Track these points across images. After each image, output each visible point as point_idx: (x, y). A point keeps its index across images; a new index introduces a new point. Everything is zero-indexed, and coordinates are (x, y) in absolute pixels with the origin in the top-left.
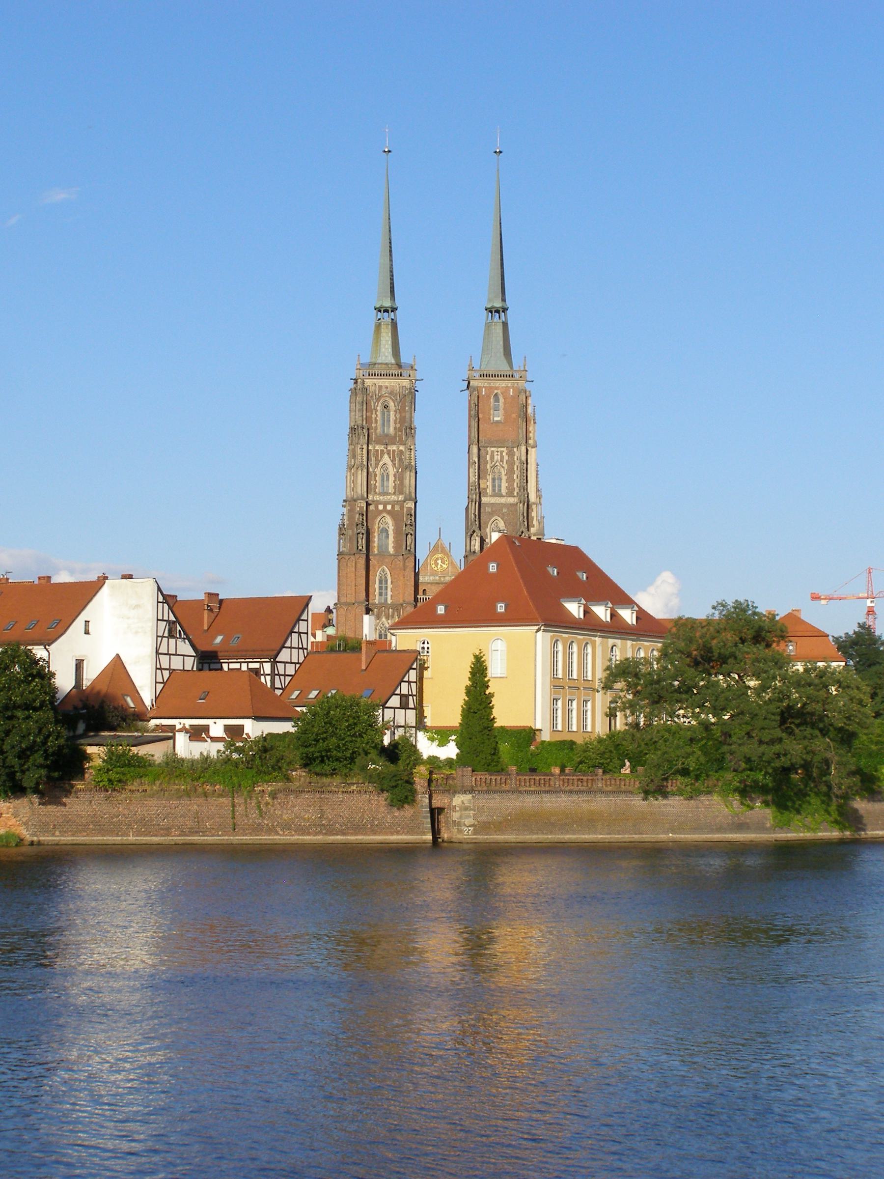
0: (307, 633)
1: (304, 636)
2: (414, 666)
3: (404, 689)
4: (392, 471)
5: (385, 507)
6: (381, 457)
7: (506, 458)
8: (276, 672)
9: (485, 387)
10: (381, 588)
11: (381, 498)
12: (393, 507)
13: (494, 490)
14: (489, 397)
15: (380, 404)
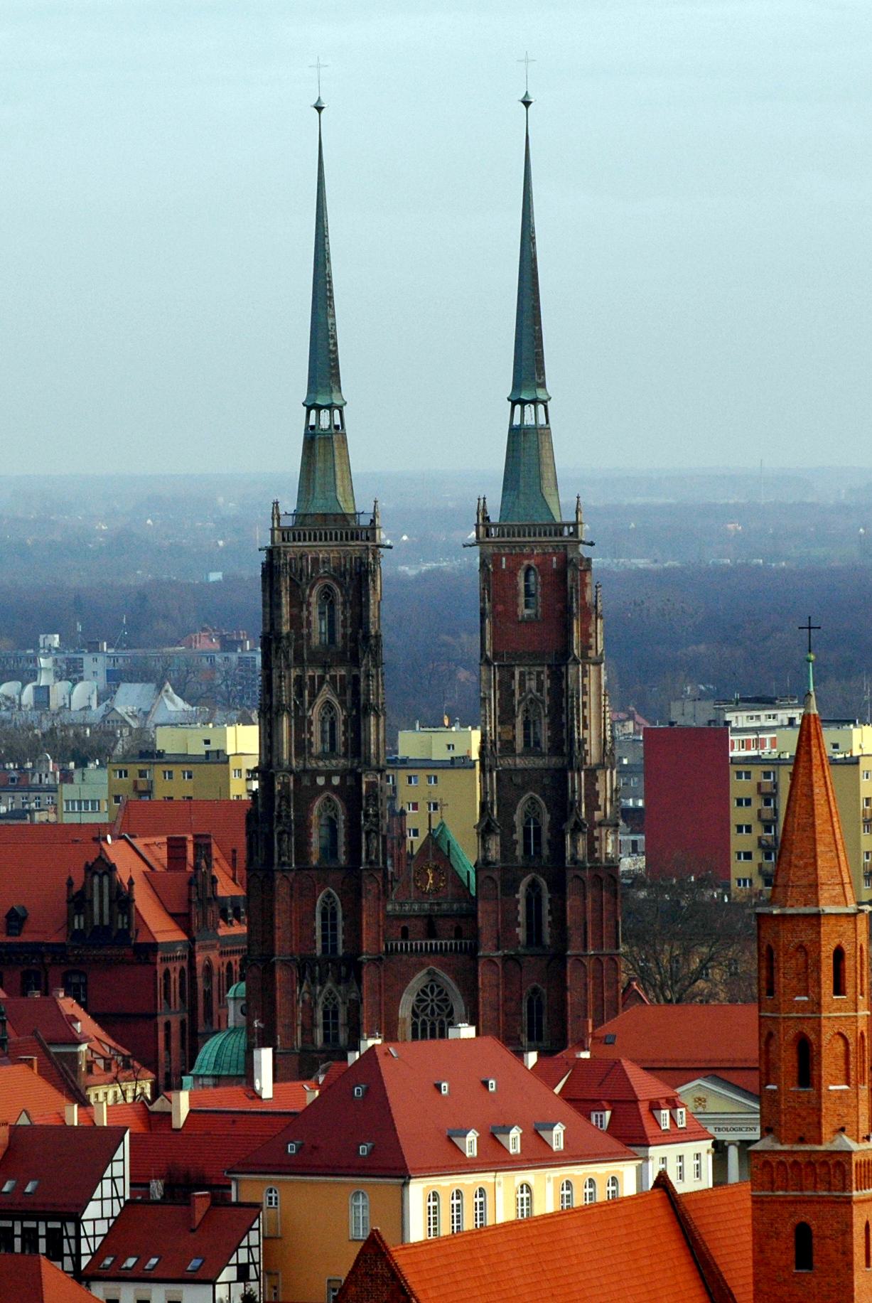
0: (123, 1177)
1: (119, 1182)
2: (256, 1225)
3: (243, 1256)
4: (341, 715)
5: (328, 781)
6: (319, 690)
7: (547, 684)
8: (83, 1234)
9: (505, 555)
10: (324, 928)
11: (321, 764)
12: (343, 779)
13: (527, 743)
14: (513, 574)
15: (314, 592)
